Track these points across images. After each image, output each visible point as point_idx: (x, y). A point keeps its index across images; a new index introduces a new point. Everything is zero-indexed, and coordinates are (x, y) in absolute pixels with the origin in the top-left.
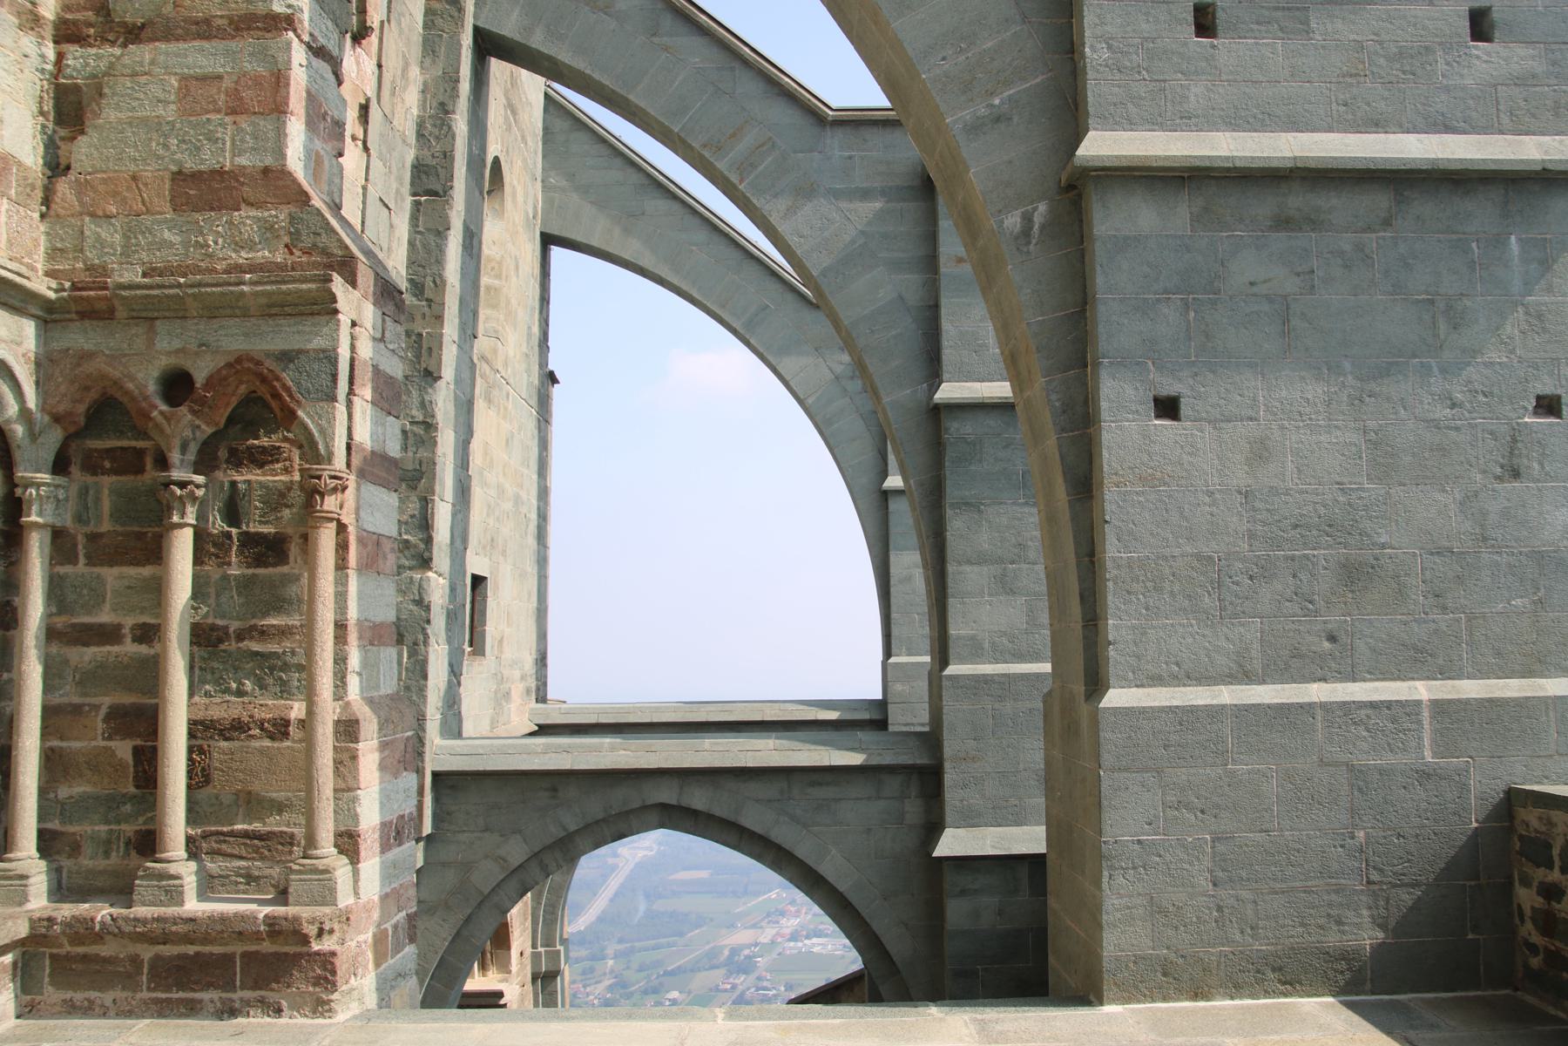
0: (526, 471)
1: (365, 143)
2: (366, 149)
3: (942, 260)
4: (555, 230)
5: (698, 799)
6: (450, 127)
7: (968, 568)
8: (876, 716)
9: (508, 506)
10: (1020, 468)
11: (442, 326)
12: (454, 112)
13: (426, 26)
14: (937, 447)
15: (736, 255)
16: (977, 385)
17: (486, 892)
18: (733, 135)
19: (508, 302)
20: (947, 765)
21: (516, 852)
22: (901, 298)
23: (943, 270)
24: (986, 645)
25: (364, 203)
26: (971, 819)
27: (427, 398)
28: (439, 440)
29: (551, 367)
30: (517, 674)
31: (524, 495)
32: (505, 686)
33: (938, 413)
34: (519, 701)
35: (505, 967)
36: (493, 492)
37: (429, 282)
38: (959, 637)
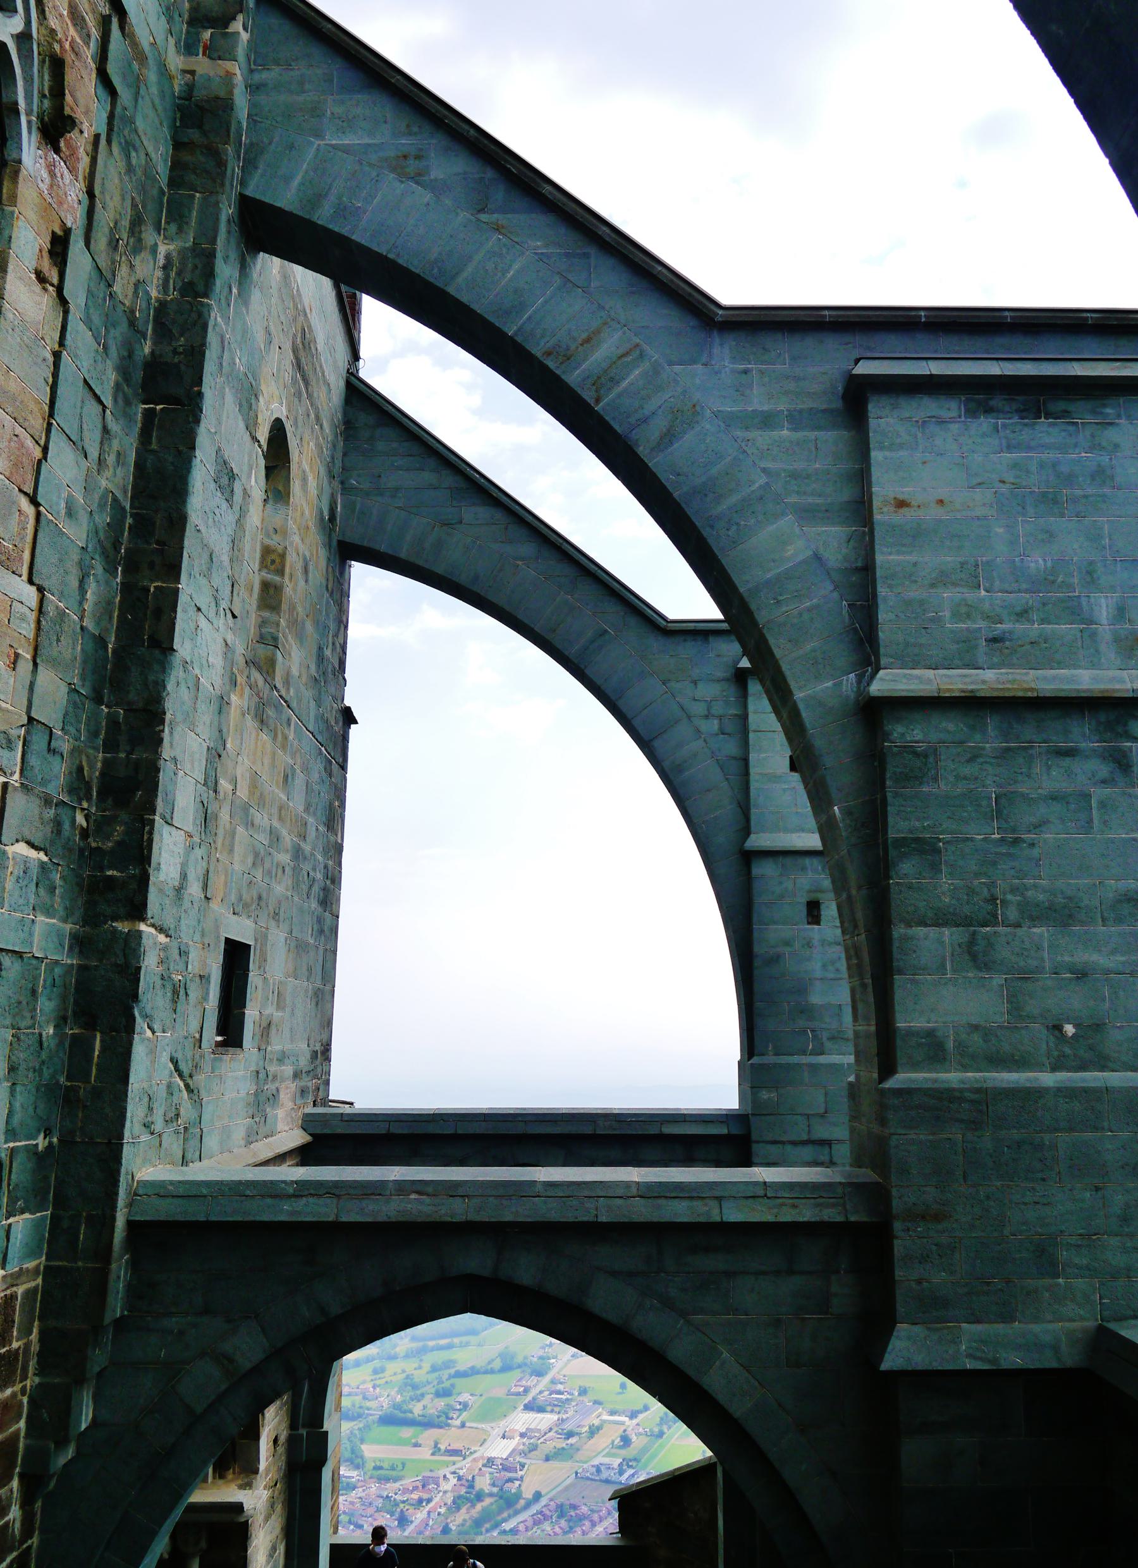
0: (311, 820)
1: (60, 289)
2: (63, 301)
3: (876, 503)
4: (354, 537)
5: (526, 1269)
6: (200, 315)
7: (920, 931)
8: (736, 1130)
9: (285, 858)
10: (993, 791)
11: (177, 579)
12: (206, 296)
13: (173, 182)
14: (873, 759)
15: (567, 570)
16: (930, 673)
17: (199, 1409)
18: (588, 340)
19: (292, 608)
20: (897, 1226)
21: (248, 1346)
22: (817, 557)
23: (877, 517)
24: (950, 1045)
25: (55, 375)
26: (935, 1309)
27: (151, 678)
28: (166, 735)
29: (347, 703)
30: (288, 1070)
31: (307, 848)
32: (271, 1087)
33: (874, 713)
34: (290, 1105)
35: (250, 1469)
36: (263, 838)
37: (159, 519)
38: (910, 1033)
